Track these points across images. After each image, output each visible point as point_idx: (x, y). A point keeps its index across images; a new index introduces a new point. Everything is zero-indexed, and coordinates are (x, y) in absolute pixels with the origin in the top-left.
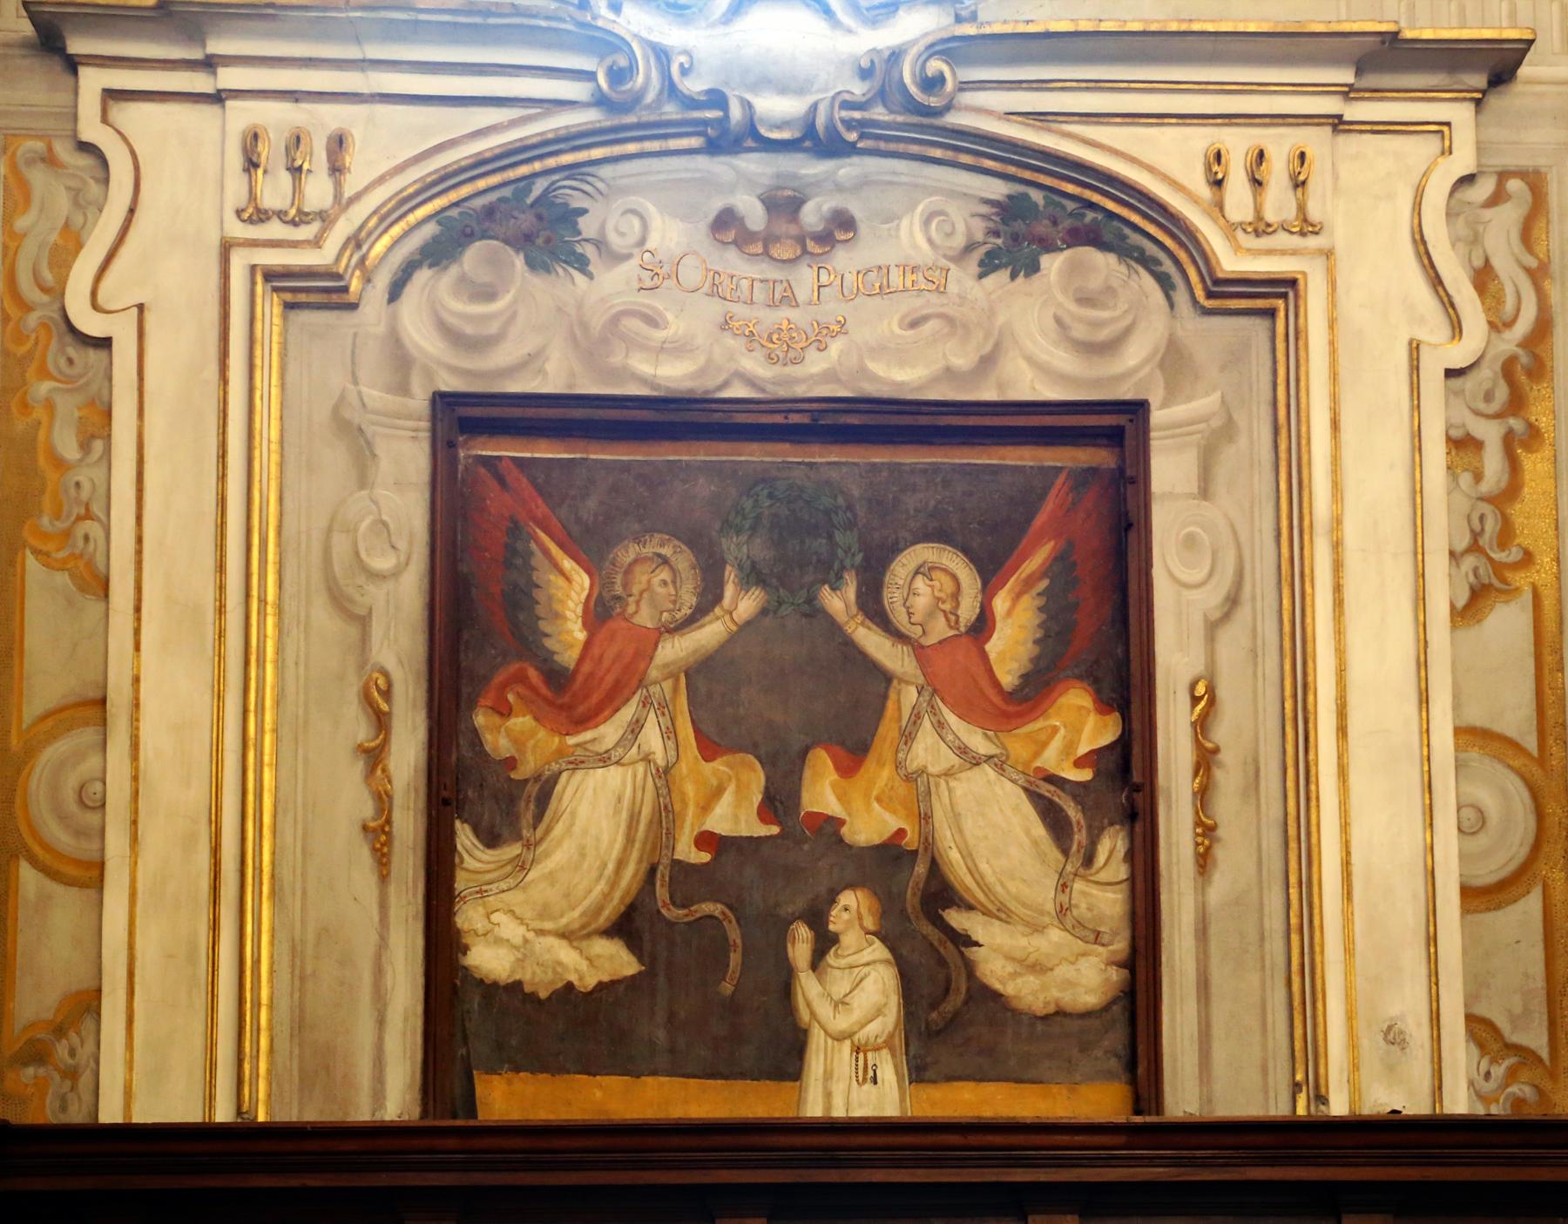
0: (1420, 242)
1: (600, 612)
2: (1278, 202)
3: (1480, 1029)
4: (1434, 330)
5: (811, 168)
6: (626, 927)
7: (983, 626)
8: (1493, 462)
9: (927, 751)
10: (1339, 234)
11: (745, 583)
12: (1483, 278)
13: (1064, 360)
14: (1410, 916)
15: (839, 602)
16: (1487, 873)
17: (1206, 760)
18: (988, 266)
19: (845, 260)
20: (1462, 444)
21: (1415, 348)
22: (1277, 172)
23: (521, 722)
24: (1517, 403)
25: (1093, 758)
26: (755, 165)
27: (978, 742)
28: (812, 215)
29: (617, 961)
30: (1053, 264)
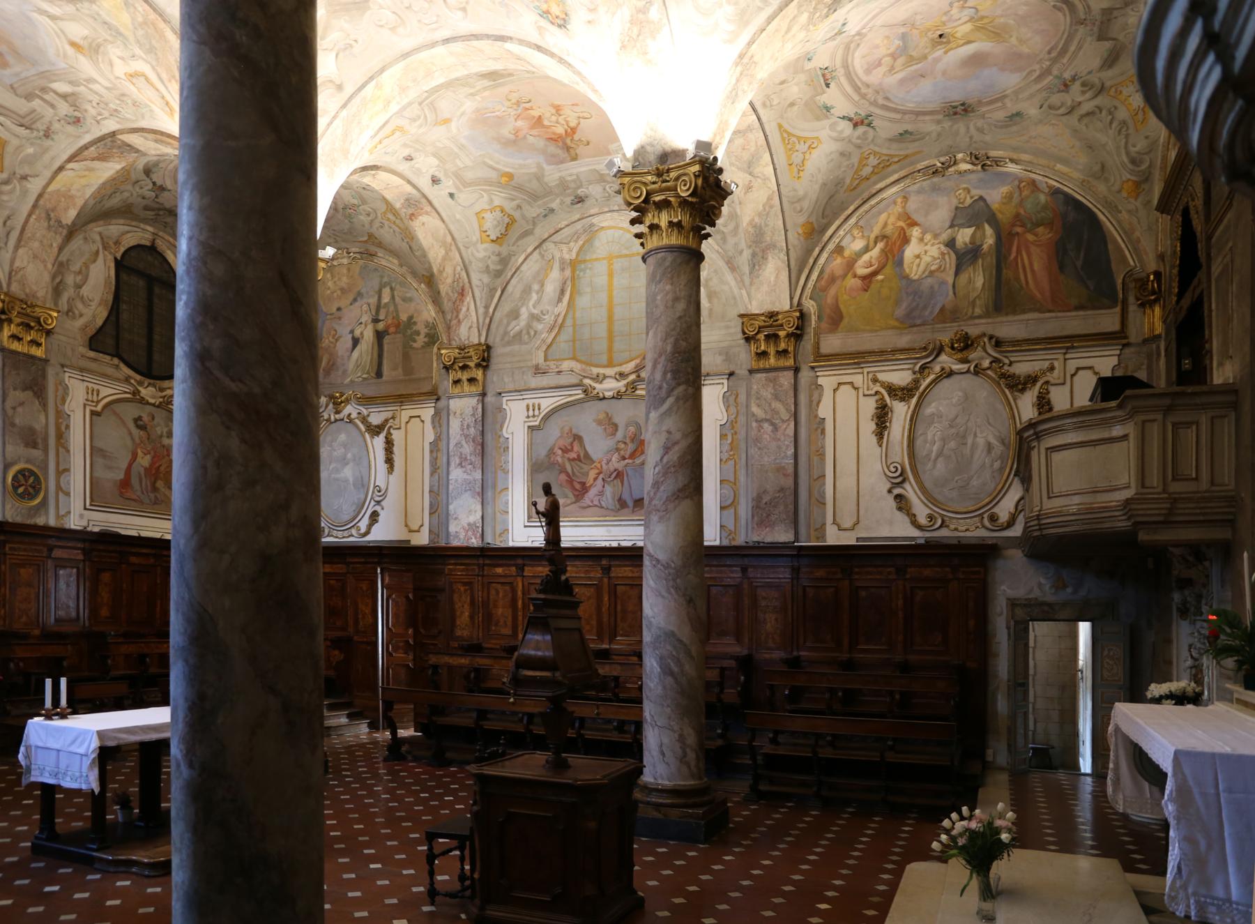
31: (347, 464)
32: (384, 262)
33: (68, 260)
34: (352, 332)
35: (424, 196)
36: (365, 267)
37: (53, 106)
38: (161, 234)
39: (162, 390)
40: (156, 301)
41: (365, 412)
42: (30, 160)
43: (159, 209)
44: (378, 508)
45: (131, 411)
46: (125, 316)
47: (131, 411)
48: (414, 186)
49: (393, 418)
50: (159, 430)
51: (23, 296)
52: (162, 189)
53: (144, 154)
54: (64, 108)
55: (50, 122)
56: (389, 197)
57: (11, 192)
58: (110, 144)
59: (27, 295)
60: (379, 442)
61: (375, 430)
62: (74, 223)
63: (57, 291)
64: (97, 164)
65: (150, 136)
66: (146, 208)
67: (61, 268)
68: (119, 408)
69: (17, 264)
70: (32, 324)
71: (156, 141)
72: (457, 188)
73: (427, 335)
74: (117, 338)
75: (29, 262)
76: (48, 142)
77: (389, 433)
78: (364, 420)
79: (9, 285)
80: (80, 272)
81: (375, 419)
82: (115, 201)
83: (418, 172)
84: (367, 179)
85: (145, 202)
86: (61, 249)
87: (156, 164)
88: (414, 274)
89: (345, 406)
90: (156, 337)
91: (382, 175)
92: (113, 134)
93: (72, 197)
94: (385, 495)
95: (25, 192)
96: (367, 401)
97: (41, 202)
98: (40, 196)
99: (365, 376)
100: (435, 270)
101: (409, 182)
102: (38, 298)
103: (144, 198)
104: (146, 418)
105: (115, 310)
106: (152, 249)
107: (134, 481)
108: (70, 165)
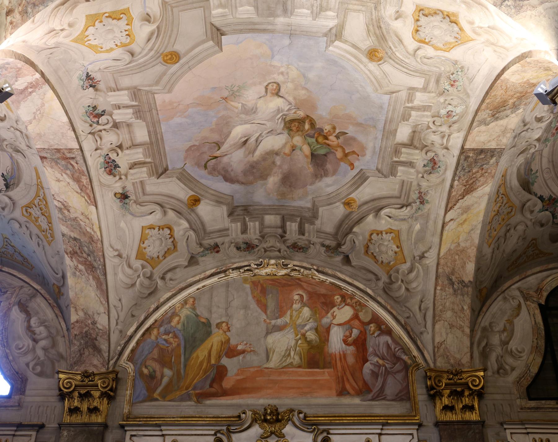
33: (490, 324)
59: (452, 366)
69: (437, 340)
75: (447, 334)
79: (435, 363)
80: (504, 330)
102: (463, 365)
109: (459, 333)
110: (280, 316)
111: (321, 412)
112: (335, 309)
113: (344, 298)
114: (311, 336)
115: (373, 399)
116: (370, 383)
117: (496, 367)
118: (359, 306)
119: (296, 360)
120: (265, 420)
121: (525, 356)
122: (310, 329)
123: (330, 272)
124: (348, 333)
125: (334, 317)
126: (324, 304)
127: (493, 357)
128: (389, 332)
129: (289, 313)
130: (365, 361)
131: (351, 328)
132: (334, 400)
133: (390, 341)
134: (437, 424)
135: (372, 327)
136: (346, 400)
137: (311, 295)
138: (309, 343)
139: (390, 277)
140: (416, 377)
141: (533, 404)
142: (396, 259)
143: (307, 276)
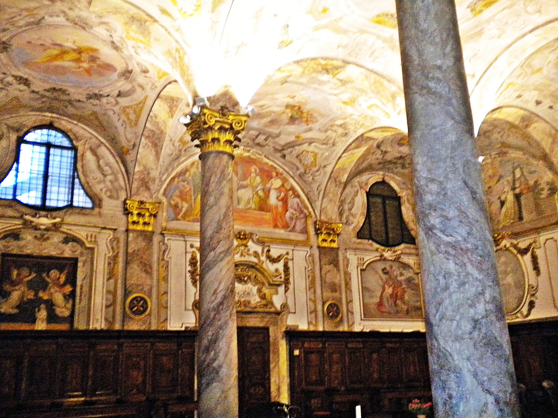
0: (106, 243)
1: (18, 275)
2: (93, 239)
3: (106, 319)
4: (107, 252)
5: (45, 232)
6: (18, 307)
7: (59, 278)
8: (112, 265)
9: (52, 290)
10: (99, 242)
11: (34, 272)
12: (112, 248)
13: (70, 253)
14: (100, 308)
15: (44, 275)
16: (109, 303)
17: (81, 293)
18: (63, 243)
19: (48, 242)
20: (109, 264)
21: (105, 255)
22: (93, 236)
23: (7, 286)
24: (115, 260)
25: (70, 292)
26: (39, 232)
27: (58, 289)
28: (46, 236)
29: (15, 311)
30: (70, 244)
31: (508, 274)
32: (513, 155)
34: (499, 198)
35: (532, 113)
36: (501, 162)
37: (335, 131)
38: (387, 174)
39: (395, 252)
40: (387, 207)
41: (515, 242)
42: (327, 158)
43: (385, 163)
44: (533, 299)
45: (380, 266)
46: (373, 218)
47: (380, 266)
48: (525, 110)
49: (535, 242)
50: (395, 273)
51: (326, 220)
52: (386, 152)
53: (377, 139)
54: (340, 131)
55: (335, 139)
56: (510, 119)
57: (320, 174)
58: (361, 140)
60: (528, 257)
61: (523, 252)
62: (346, 181)
63: (341, 214)
64: (355, 151)
65: (379, 130)
66: (379, 163)
67: (342, 202)
68: (374, 265)
69: (323, 206)
70: (331, 232)
71: (383, 131)
72: (555, 103)
73: (550, 189)
74: (370, 231)
76: (335, 148)
77: (533, 252)
78: (515, 247)
79: (320, 216)
81: (523, 245)
82: (364, 165)
83: (527, 102)
84: (496, 115)
85: (377, 161)
86: (342, 194)
87: (382, 142)
88: (534, 156)
89: (501, 242)
90: (390, 225)
91: (504, 110)
92: (362, 135)
93: (345, 169)
94: (536, 290)
95: (325, 173)
96: (516, 235)
97: (332, 175)
98: (332, 172)
99: (512, 221)
100: (547, 151)
101: (522, 108)
103: (378, 159)
104: (388, 268)
105: (368, 217)
106: (383, 182)
107: (385, 300)
108: (344, 155)
109: (333, 203)
110: (245, 180)
111: (266, 235)
112: (273, 179)
113: (277, 174)
114: (261, 193)
115: (290, 231)
116: (289, 222)
117: (345, 221)
118: (284, 180)
119: (253, 206)
120: (239, 238)
121: (358, 216)
122: (260, 189)
123: (271, 158)
124: (279, 194)
125: (272, 184)
126: (267, 176)
127: (345, 216)
128: (298, 196)
129: (249, 179)
130: (287, 211)
131: (280, 192)
132: (271, 229)
133: (299, 202)
134: (319, 247)
135: (291, 193)
136: (277, 231)
137: (262, 170)
138: (260, 197)
139: (306, 171)
140: (310, 222)
141: (359, 240)
142: (312, 164)
143: (259, 158)
